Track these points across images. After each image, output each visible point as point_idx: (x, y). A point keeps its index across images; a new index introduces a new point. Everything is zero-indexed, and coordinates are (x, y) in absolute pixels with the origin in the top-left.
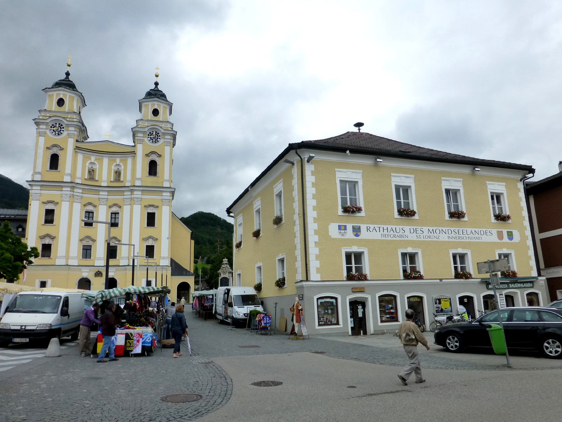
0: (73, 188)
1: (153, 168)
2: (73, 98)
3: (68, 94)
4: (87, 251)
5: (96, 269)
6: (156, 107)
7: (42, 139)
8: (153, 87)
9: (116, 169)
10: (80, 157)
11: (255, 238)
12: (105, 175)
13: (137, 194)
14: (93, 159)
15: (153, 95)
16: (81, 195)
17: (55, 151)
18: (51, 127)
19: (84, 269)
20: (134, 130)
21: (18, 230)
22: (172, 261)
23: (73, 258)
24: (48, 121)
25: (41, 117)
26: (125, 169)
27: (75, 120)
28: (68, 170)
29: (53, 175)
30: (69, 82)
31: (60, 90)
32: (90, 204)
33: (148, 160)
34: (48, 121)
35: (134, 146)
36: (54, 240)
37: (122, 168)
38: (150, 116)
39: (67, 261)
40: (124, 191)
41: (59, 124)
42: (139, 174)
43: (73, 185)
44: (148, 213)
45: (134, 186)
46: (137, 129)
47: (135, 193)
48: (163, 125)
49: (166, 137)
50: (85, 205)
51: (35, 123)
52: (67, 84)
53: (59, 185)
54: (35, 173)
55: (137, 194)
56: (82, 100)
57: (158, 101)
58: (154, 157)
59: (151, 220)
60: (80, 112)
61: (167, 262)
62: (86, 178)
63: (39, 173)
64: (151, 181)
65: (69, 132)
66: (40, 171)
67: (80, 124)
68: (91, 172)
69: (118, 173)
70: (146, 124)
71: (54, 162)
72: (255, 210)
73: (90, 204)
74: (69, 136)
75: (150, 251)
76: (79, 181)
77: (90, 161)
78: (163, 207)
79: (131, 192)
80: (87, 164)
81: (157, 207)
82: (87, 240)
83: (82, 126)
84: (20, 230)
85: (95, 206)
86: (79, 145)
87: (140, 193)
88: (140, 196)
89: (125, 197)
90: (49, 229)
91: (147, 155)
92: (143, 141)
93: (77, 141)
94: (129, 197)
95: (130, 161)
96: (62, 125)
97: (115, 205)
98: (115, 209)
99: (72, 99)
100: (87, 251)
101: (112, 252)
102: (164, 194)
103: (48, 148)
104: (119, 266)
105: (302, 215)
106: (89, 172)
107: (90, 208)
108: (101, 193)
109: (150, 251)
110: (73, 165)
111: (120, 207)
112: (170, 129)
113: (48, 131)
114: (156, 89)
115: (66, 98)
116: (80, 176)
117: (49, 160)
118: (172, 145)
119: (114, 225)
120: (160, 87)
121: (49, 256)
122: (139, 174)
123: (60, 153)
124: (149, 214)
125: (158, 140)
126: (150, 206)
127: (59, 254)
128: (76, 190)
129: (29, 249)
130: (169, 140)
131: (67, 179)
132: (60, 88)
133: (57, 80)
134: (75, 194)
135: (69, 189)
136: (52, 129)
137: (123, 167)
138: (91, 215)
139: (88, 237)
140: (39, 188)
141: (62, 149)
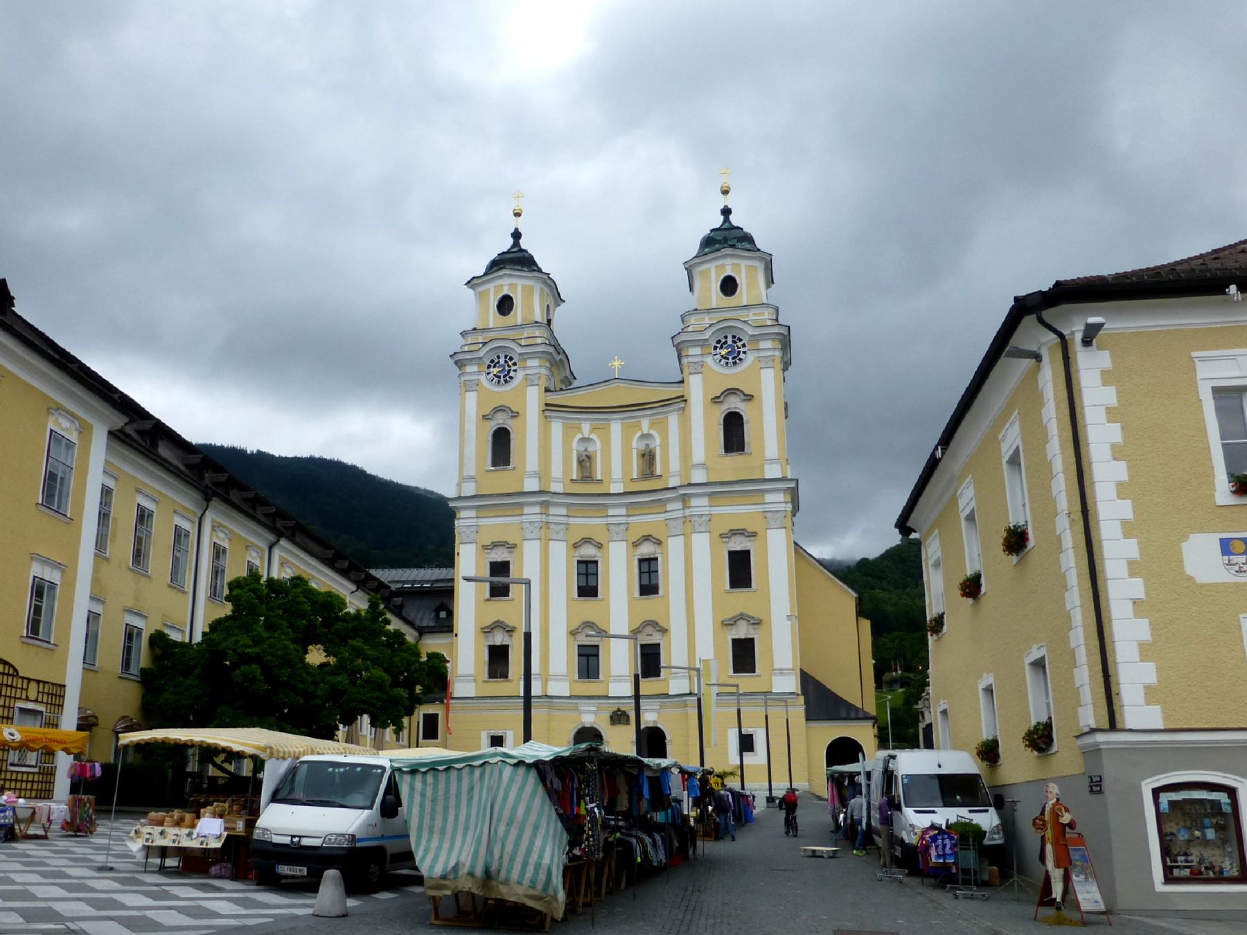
0: (546, 505)
1: (734, 433)
2: (531, 289)
3: (520, 283)
4: (589, 661)
5: (613, 706)
6: (729, 272)
8: (718, 221)
9: (642, 447)
10: (557, 427)
11: (970, 601)
13: (700, 504)
14: (586, 428)
15: (719, 242)
16: (564, 520)
17: (500, 420)
18: (489, 367)
20: (678, 340)
21: (437, 615)
22: (807, 681)
23: (558, 678)
24: (481, 354)
25: (466, 349)
27: (539, 341)
28: (532, 463)
29: (501, 481)
30: (520, 254)
31: (501, 277)
32: (587, 541)
33: (719, 413)
34: (481, 354)
35: (682, 382)
38: (715, 297)
42: (698, 455)
44: (731, 553)
45: (690, 485)
46: (684, 337)
47: (694, 502)
48: (751, 316)
51: (456, 363)
53: (512, 501)
54: (464, 479)
55: (700, 504)
57: (733, 256)
58: (734, 404)
59: (740, 569)
60: (549, 321)
61: (790, 684)
63: (471, 478)
64: (732, 466)
65: (529, 372)
66: (472, 473)
67: (551, 350)
68: (585, 461)
69: (648, 458)
70: (707, 320)
71: (501, 445)
72: (963, 516)
73: (587, 541)
75: (744, 655)
76: (557, 487)
77: (580, 436)
79: (683, 501)
80: (574, 444)
81: (754, 535)
83: (555, 354)
84: (443, 614)
85: (599, 546)
86: (554, 398)
87: (705, 501)
88: (706, 510)
90: (501, 610)
91: (716, 400)
92: (702, 364)
93: (547, 390)
94: (680, 514)
95: (673, 420)
97: (647, 538)
98: (646, 550)
99: (528, 291)
100: (589, 661)
101: (650, 661)
102: (769, 498)
104: (667, 696)
105: (1078, 516)
106: (580, 462)
107: (588, 552)
108: (611, 512)
109: (744, 655)
110: (544, 450)
111: (659, 543)
112: (769, 323)
113: (483, 378)
114: (726, 225)
115: (516, 294)
118: (779, 365)
119: (649, 588)
120: (735, 220)
123: (511, 425)
125: (742, 356)
126: (734, 533)
128: (553, 510)
129: (332, 660)
130: (770, 353)
131: (531, 485)
132: (501, 273)
133: (493, 255)
134: (551, 519)
135: (537, 509)
137: (658, 441)
138: (591, 568)
139: (588, 624)
140: (473, 513)
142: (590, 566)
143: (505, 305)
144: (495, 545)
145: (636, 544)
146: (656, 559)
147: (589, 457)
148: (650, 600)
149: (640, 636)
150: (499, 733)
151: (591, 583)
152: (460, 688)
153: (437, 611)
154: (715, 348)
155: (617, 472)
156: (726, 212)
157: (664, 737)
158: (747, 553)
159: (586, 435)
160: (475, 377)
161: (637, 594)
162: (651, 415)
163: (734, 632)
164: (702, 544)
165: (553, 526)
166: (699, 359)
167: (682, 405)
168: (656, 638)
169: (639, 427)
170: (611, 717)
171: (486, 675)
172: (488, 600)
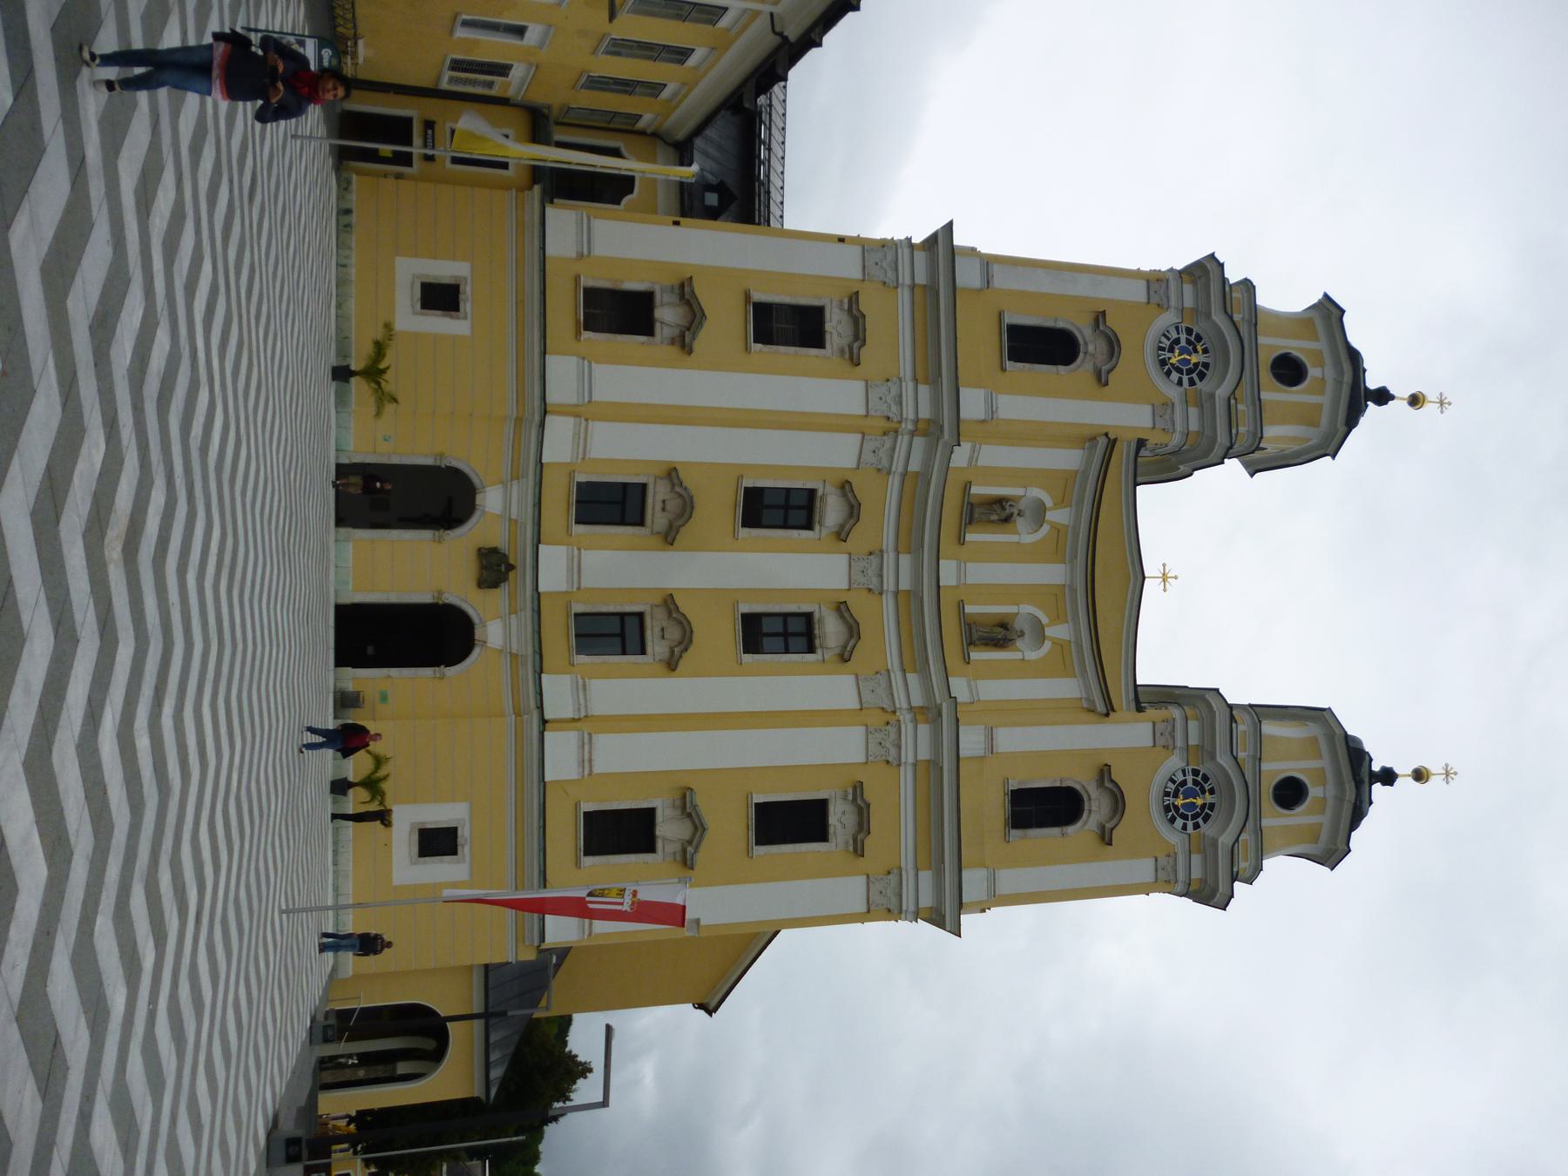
1: (1043, 807)
2: (1313, 423)
3: (1325, 400)
5: (520, 556)
6: (1314, 792)
7: (1138, 293)
9: (1018, 624)
12: (993, 572)
13: (917, 743)
16: (898, 466)
17: (1092, 346)
19: (520, 494)
21: (709, 187)
23: (581, 440)
26: (1025, 670)
28: (1013, 407)
29: (979, 341)
33: (1080, 778)
34: (1218, 318)
36: (674, 351)
37: (1024, 651)
39: (564, 411)
40: (924, 670)
41: (1206, 365)
42: (1011, 739)
43: (942, 430)
47: (924, 730)
49: (1196, 859)
50: (845, 487)
52: (1359, 397)
55: (917, 743)
56: (1285, 457)
58: (1097, 808)
62: (975, 490)
64: (985, 804)
66: (997, 282)
68: (999, 511)
69: (999, 634)
71: (1039, 347)
74: (1162, 409)
78: (860, 881)
80: (1036, 492)
81: (859, 851)
82: (674, 505)
84: (712, 199)
85: (841, 535)
88: (908, 756)
89: (897, 677)
91: (1104, 774)
92: (1169, 748)
93: (1141, 443)
94: (901, 702)
96: (1202, 376)
98: (831, 630)
100: (610, 504)
101: (612, 633)
103: (1099, 318)
104: (539, 672)
106: (1000, 502)
107: (832, 511)
109: (620, 831)
111: (844, 657)
116: (990, 463)
117: (1049, 324)
121: (591, 324)
122: (1011, 739)
123: (1080, 373)
124: (821, 806)
127: (600, 371)
131: (973, 404)
134: (903, 441)
135: (925, 413)
136: (1183, 337)
137: (1032, 655)
138: (797, 516)
139: (687, 507)
141: (1101, 379)
142: (804, 513)
143: (1289, 370)
144: (857, 321)
145: (842, 609)
146: (811, 649)
147: (1007, 520)
148: (729, 634)
149: (661, 614)
150: (466, 305)
151: (767, 515)
152: (565, 224)
153: (720, 188)
154: (1196, 772)
155: (982, 573)
156: (1388, 777)
157: (449, 664)
158: (818, 832)
159: (1049, 516)
160: (1173, 302)
161: (745, 608)
162: (1079, 646)
163: (669, 812)
164: (843, 747)
165: (888, 444)
166: (1179, 743)
167: (1101, 707)
168: (657, 647)
169: (1058, 618)
170: (494, 551)
171: (591, 283)
172: (747, 296)
